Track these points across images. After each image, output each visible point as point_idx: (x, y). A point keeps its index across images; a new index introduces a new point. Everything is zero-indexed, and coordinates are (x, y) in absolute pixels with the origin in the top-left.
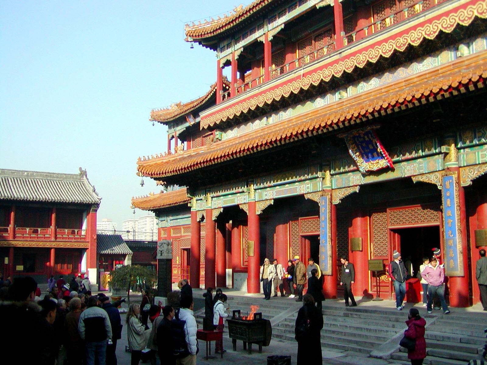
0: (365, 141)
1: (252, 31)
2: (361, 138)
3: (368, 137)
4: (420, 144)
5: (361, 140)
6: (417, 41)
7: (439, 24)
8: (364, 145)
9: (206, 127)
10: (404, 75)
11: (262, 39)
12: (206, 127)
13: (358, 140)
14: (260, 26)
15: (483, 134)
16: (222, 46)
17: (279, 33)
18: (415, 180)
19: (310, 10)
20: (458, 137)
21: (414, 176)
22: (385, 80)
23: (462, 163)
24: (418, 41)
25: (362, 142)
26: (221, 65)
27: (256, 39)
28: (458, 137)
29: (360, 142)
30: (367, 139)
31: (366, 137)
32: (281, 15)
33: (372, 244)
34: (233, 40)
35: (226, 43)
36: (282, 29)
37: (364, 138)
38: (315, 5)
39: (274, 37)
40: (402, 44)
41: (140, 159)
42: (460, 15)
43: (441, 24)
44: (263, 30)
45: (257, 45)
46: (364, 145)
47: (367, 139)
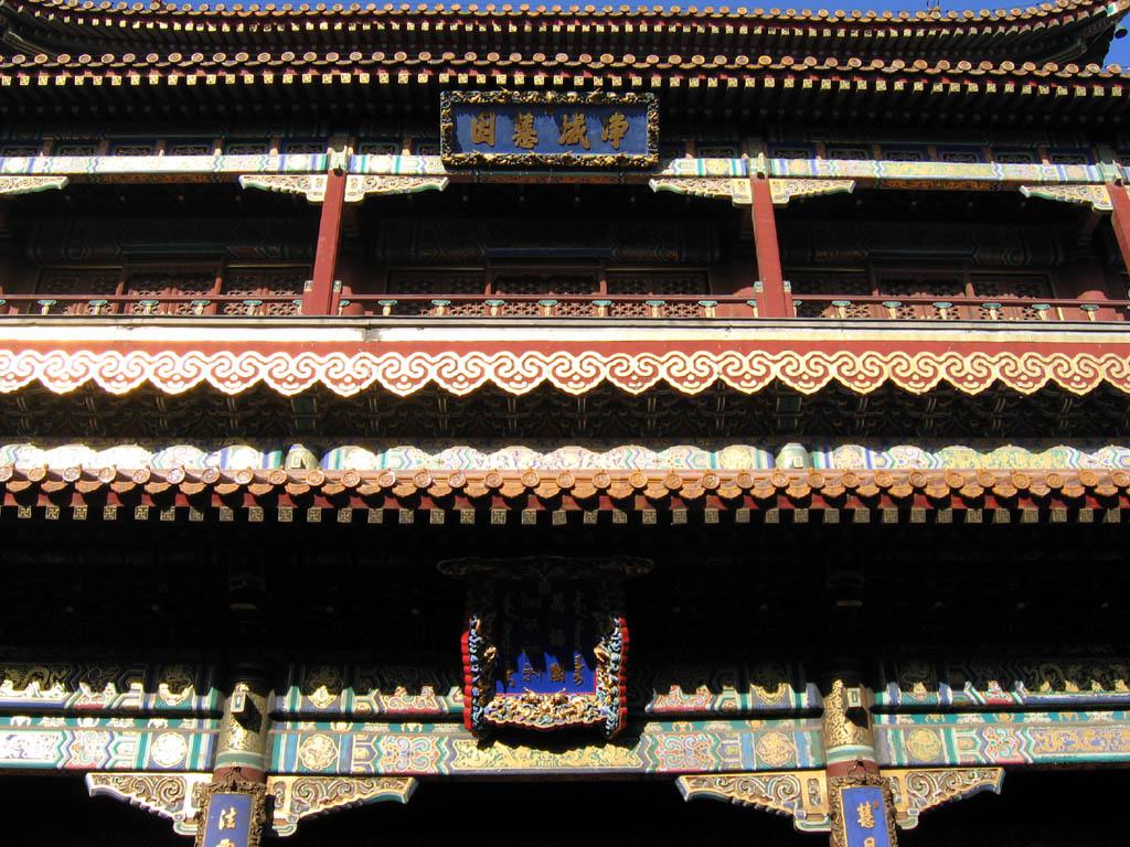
7: (775, 362)
19: (205, 180)
23: (893, 754)
38: (238, 174)
40: (634, 373)
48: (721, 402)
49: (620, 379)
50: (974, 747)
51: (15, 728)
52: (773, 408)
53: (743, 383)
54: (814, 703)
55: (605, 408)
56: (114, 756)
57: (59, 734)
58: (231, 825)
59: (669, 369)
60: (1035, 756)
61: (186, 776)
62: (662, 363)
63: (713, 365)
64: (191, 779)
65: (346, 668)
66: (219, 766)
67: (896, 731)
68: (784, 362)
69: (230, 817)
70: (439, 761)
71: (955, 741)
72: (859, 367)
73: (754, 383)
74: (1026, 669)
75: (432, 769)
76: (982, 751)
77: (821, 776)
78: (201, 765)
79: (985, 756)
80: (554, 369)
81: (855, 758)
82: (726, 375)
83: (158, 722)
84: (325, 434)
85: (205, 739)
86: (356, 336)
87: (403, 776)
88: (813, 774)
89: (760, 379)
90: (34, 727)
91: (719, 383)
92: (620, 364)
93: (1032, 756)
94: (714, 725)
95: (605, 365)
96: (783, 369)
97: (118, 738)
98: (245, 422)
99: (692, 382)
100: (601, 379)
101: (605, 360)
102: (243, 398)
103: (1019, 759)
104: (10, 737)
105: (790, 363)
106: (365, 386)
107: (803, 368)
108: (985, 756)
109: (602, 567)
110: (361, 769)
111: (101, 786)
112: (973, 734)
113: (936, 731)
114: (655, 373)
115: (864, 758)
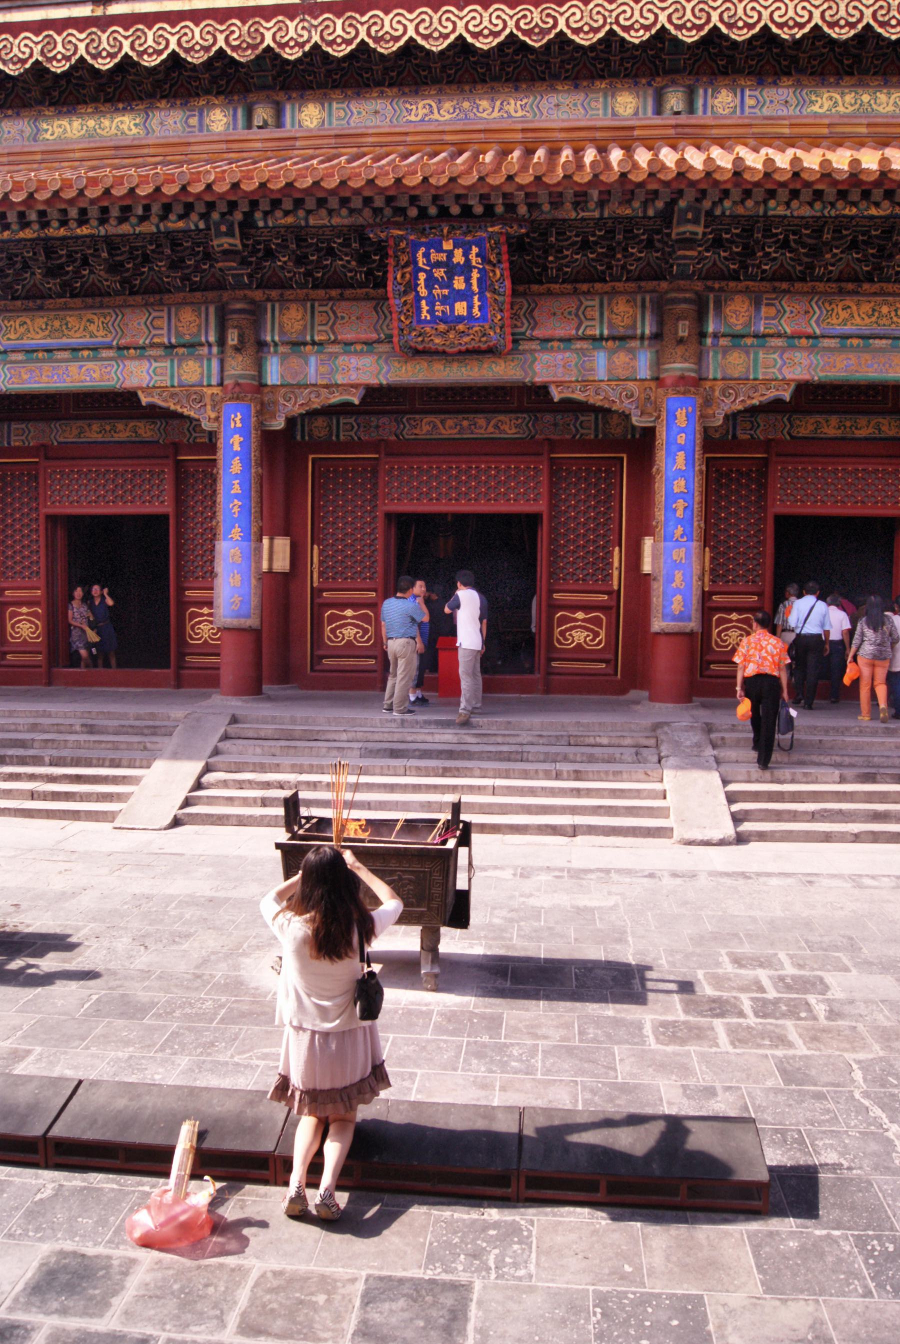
2: (440, 250)
3: (466, 254)
4: (596, 303)
5: (443, 257)
6: (637, 31)
7: (663, 9)
10: (496, 114)
13: (426, 255)
15: (779, 311)
18: (556, 394)
20: (711, 306)
21: (558, 384)
22: (426, 111)
23: (711, 371)
24: (641, 32)
25: (438, 264)
28: (711, 306)
29: (429, 263)
30: (458, 257)
33: (316, 547)
37: (450, 254)
40: (537, 25)
42: (520, 15)
43: (719, 11)
46: (439, 273)
47: (458, 257)
48: (615, 47)
49: (525, 32)
50: (774, 366)
51: (83, 359)
52: (662, 49)
53: (632, 33)
54: (654, 330)
55: (516, 53)
57: (114, 363)
58: (239, 425)
59: (567, 20)
60: (821, 374)
61: (205, 389)
62: (562, 14)
63: (607, 14)
64: (209, 391)
65: (309, 304)
66: (226, 382)
67: (716, 353)
68: (671, 10)
69: (238, 419)
70: (379, 373)
71: (761, 360)
72: (740, 12)
73: (641, 32)
74: (827, 305)
75: (374, 381)
76: (780, 370)
77: (653, 385)
78: (214, 382)
79: (781, 373)
80: (468, 23)
81: (678, 373)
82: (617, 22)
83: (181, 351)
84: (281, 89)
85: (215, 364)
87: (355, 386)
88: (647, 384)
89: (647, 28)
90: (95, 359)
91: (611, 32)
92: (525, 17)
93: (818, 375)
94: (579, 345)
95: (511, 17)
96: (669, 18)
97: (155, 365)
98: (214, 80)
99: (587, 33)
100: (507, 31)
101: (511, 13)
102: (209, 64)
103: (807, 377)
104: (81, 367)
105: (676, 10)
106: (307, 48)
107: (688, 15)
108: (781, 373)
109: (490, 229)
110: (325, 382)
111: (150, 400)
112: (775, 356)
113: (747, 353)
114: (555, 25)
115: (687, 374)
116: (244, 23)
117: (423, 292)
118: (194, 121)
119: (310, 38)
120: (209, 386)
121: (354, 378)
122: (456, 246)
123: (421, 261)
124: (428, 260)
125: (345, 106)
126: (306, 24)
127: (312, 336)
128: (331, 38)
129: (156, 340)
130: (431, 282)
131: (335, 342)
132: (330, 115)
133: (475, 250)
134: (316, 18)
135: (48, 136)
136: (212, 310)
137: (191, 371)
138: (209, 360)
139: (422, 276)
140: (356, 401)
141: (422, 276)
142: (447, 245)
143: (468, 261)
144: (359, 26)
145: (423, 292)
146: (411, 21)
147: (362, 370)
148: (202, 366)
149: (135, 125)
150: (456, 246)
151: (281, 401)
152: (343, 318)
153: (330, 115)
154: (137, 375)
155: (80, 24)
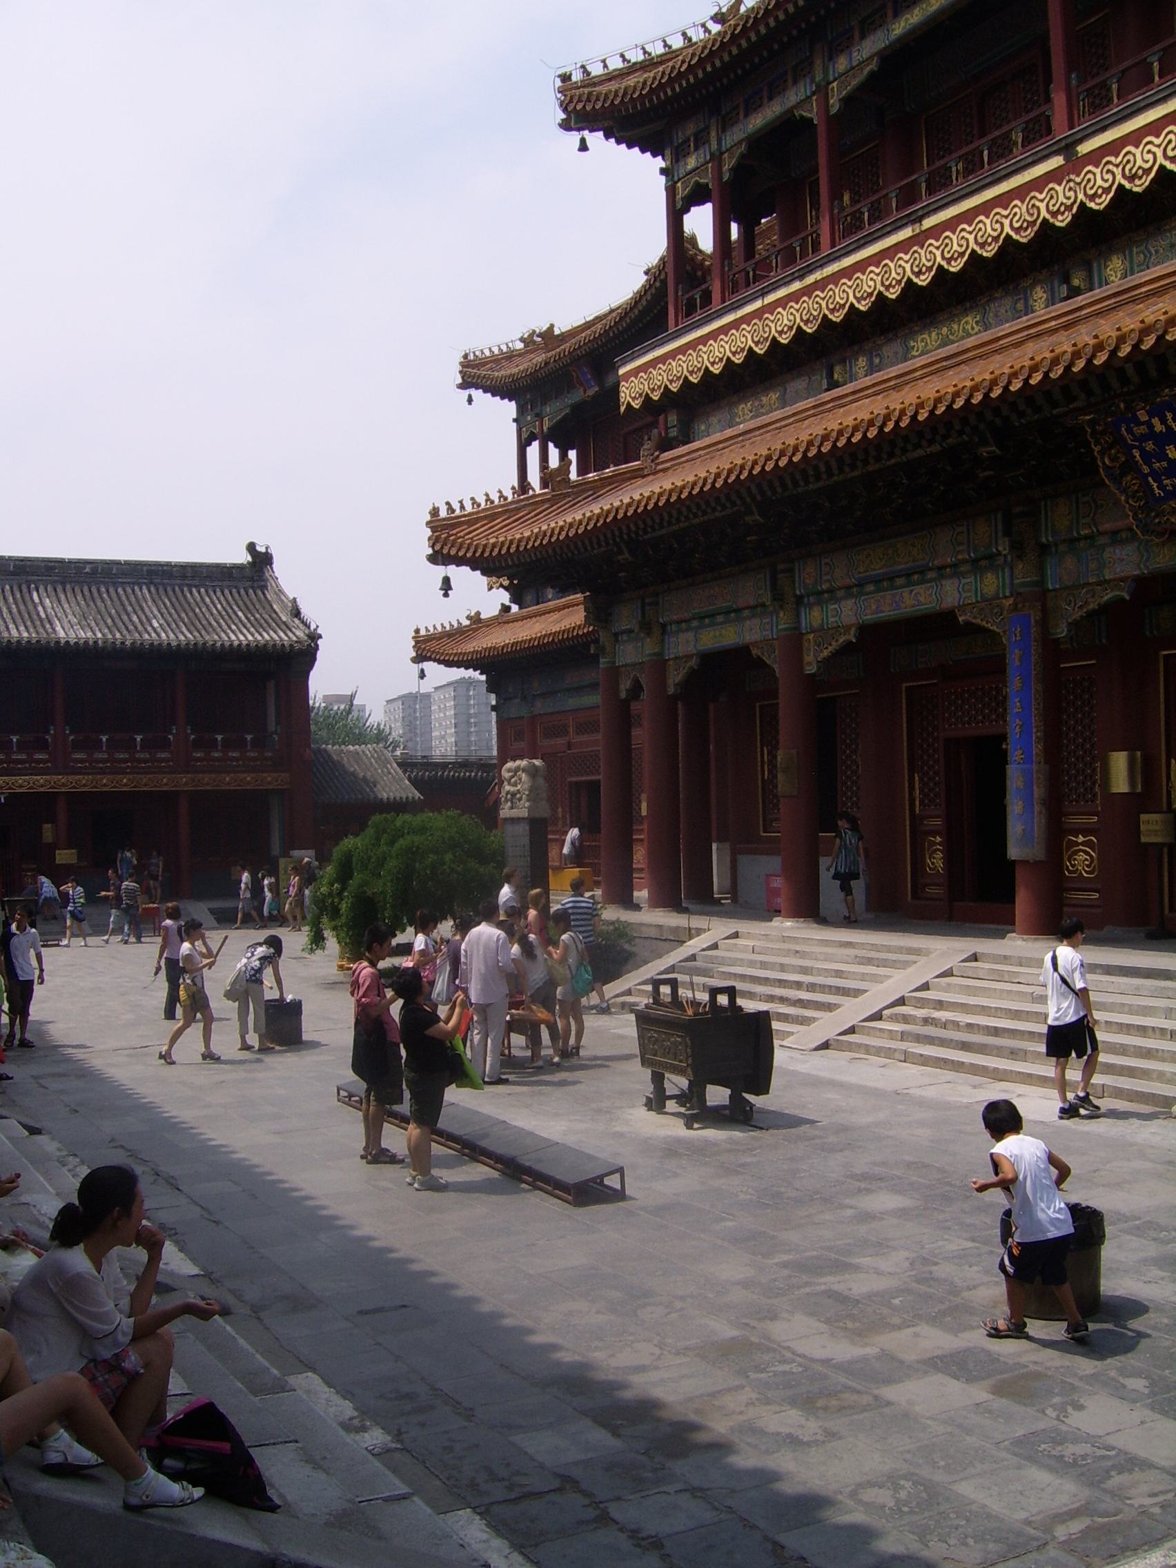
0: (1151, 435)
1: (775, 90)
2: (1139, 423)
3: (1163, 421)
5: (1143, 429)
8: (1150, 446)
9: (636, 404)
11: (812, 112)
12: (636, 404)
13: (1129, 431)
14: (801, 71)
16: (679, 137)
17: (861, 88)
25: (1143, 438)
26: (679, 205)
27: (790, 111)
31: (1156, 421)
32: (868, 26)
34: (713, 120)
35: (690, 129)
36: (872, 75)
37: (1150, 426)
39: (847, 101)
41: (435, 512)
44: (812, 81)
45: (791, 128)
47: (1159, 427)
56: (964, 595)
83: (983, 563)
86: (1056, 162)
87: (1123, 580)
97: (963, 581)
116: (1023, 202)
117: (1146, 470)
118: (1020, 306)
119: (1076, 197)
120: (1006, 597)
121: (1121, 570)
122: (1151, 415)
123: (1129, 438)
124: (1133, 434)
125: (1143, 248)
126: (1072, 184)
127: (1078, 533)
128: (1055, 209)
129: (960, 557)
130: (1147, 457)
131: (1100, 533)
132: (1131, 262)
133: (1169, 416)
134: (1078, 175)
135: (914, 353)
136: (999, 516)
137: (990, 583)
138: (1003, 570)
139: (1136, 453)
140: (1128, 598)
141: (1136, 453)
142: (1143, 416)
143: (1169, 428)
144: (1115, 169)
145: (1146, 470)
146: (1159, 146)
147: (1125, 563)
148: (997, 578)
149: (977, 323)
150: (1151, 415)
151: (1064, 605)
152: (1102, 506)
153: (1131, 262)
154: (948, 594)
155: (903, 246)
